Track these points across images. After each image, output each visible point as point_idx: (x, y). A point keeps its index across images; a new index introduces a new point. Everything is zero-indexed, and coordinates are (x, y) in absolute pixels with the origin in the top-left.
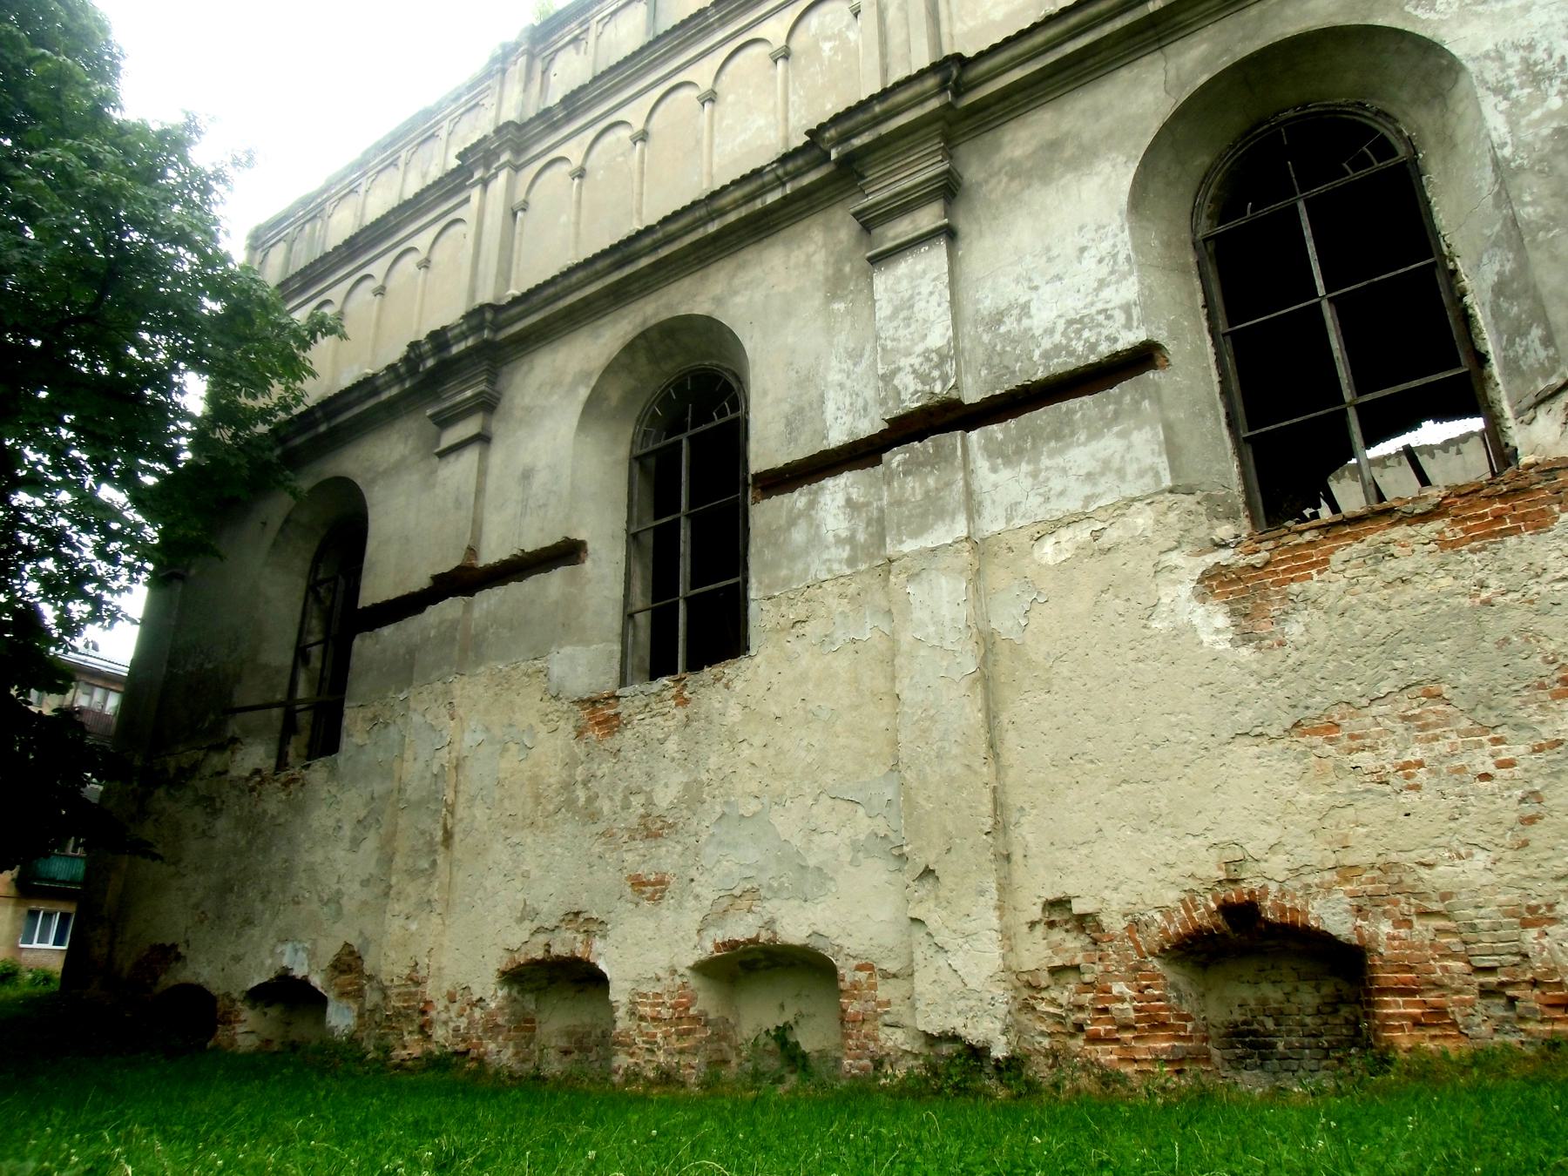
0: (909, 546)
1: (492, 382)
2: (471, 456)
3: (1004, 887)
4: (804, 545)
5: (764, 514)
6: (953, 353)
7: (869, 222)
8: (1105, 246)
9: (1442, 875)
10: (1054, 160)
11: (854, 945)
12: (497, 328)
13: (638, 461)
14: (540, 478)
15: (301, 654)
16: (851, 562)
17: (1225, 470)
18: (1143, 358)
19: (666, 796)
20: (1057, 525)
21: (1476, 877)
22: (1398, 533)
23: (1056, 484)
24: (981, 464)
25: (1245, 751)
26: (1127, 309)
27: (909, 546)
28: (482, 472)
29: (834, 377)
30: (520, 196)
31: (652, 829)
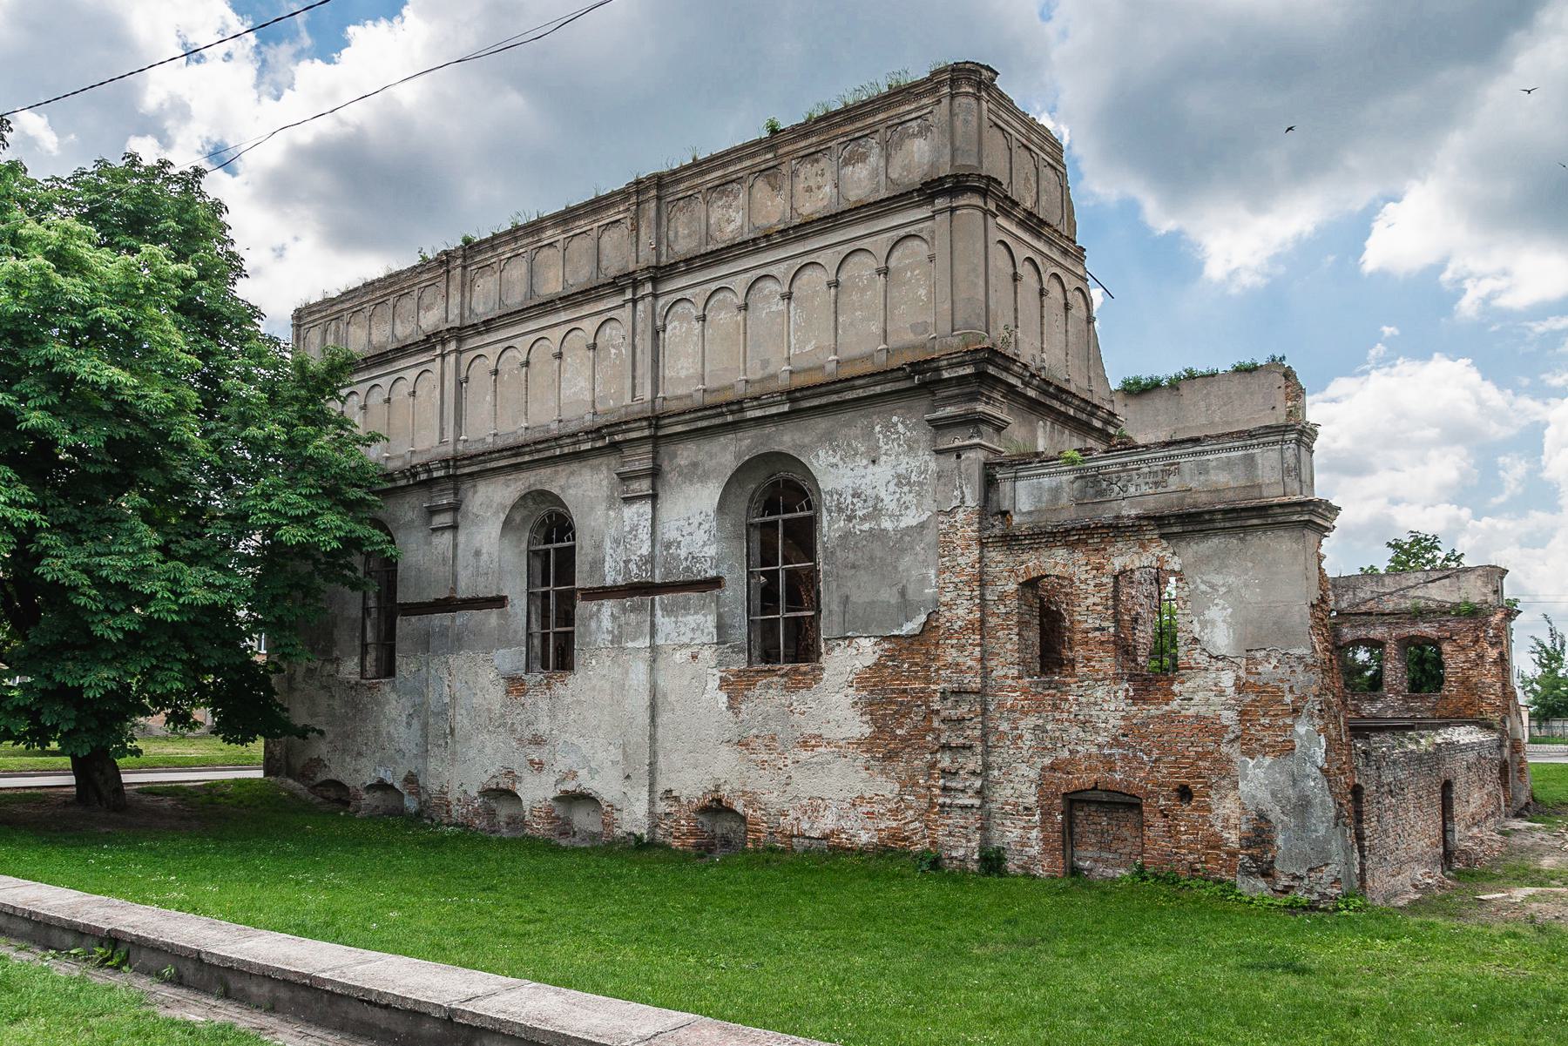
0: (630, 645)
1: (456, 492)
2: (448, 536)
3: (652, 785)
4: (600, 621)
5: (582, 607)
6: (651, 559)
7: (624, 478)
8: (706, 526)
9: (765, 798)
10: (694, 473)
11: (606, 797)
12: (456, 467)
13: (532, 554)
14: (484, 557)
15: (366, 610)
16: (612, 642)
17: (740, 634)
18: (716, 583)
19: (543, 727)
20: (681, 646)
21: (773, 798)
22: (775, 679)
23: (683, 629)
24: (659, 613)
25: (725, 748)
26: (712, 558)
27: (630, 645)
28: (455, 546)
29: (609, 551)
30: (463, 375)
31: (537, 741)
